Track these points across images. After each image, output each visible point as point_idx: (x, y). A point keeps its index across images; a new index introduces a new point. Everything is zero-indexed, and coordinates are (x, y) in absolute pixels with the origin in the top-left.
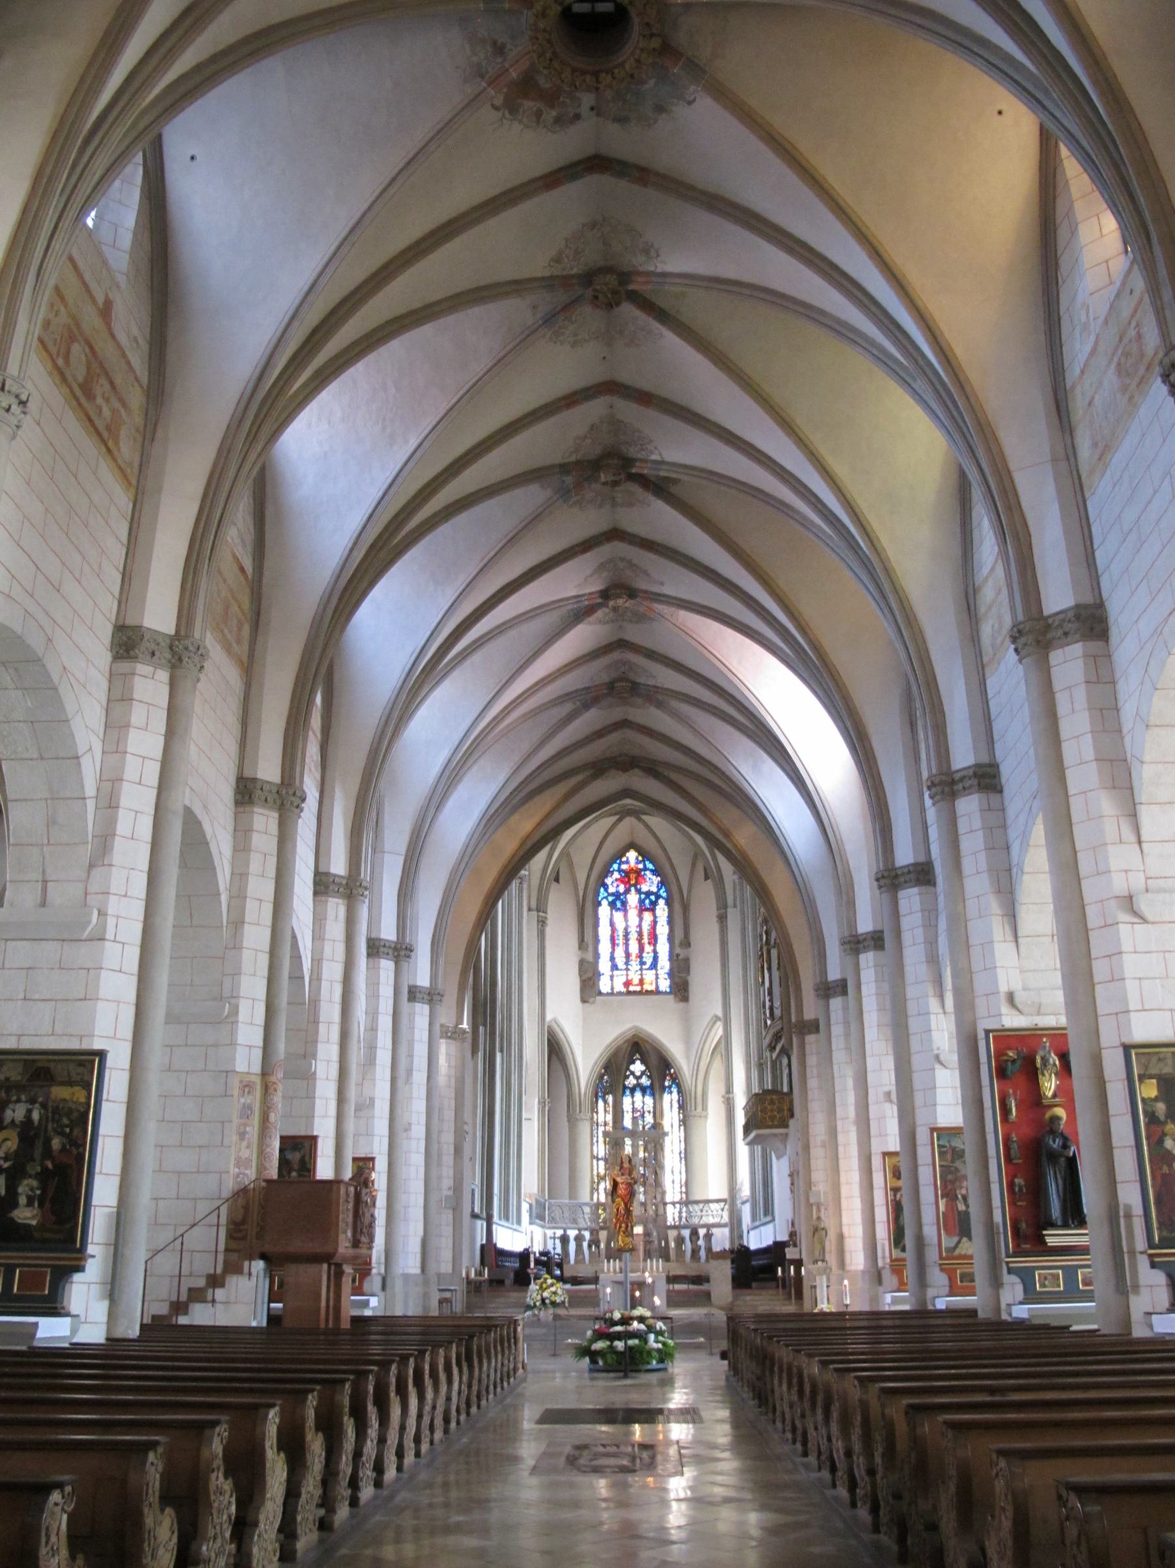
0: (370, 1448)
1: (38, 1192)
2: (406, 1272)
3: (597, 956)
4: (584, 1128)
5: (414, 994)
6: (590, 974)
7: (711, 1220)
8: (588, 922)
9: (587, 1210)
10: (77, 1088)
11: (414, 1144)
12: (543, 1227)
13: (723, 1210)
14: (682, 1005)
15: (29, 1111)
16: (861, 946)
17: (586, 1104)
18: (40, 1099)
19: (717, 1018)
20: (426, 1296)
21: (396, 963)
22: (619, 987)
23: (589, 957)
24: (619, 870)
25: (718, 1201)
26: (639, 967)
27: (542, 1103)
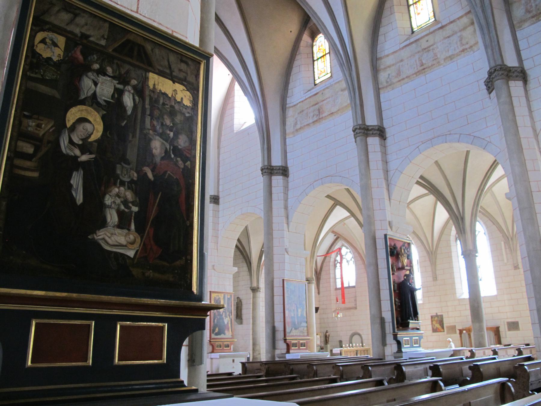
1: (135, 209)
15: (119, 93)
18: (134, 82)
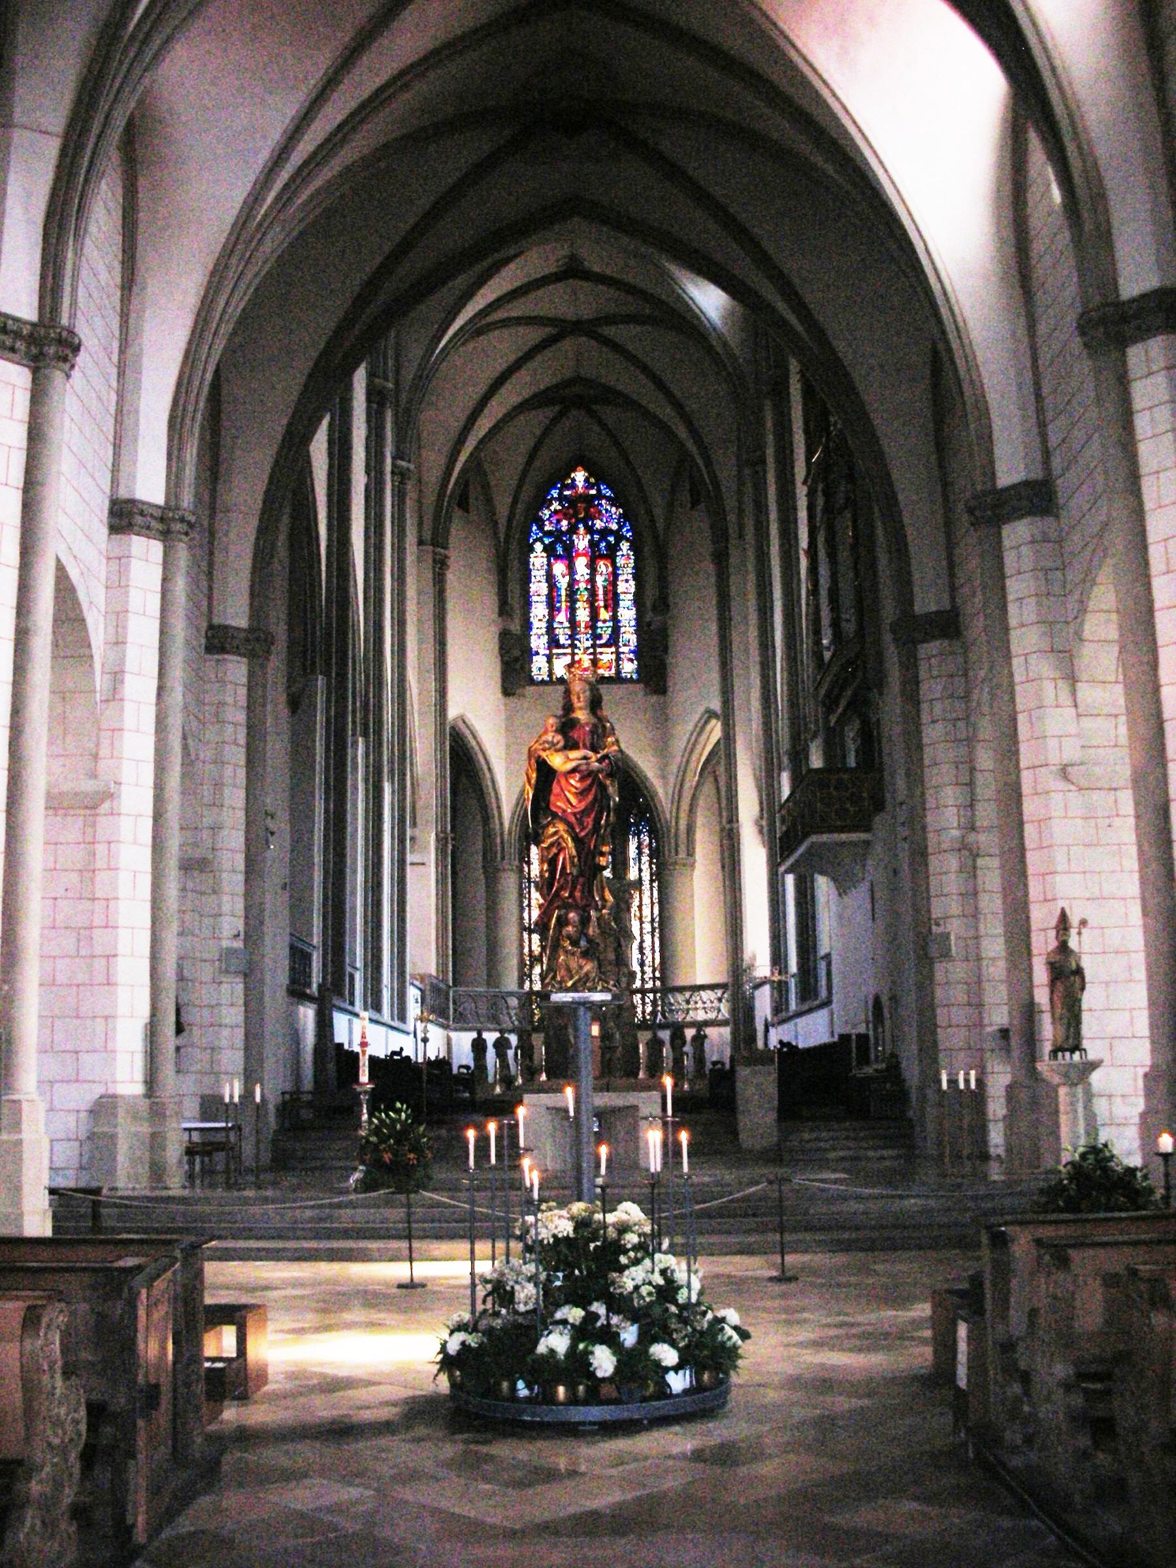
2: (110, 1092)
3: (527, 626)
4: (509, 882)
6: (516, 653)
7: (701, 1016)
8: (513, 575)
9: (514, 1002)
11: (126, 826)
12: (445, 1027)
13: (720, 1000)
14: (654, 699)
16: (1128, 330)
17: (512, 850)
19: (711, 714)
20: (156, 1142)
21: (35, 371)
22: (560, 670)
23: (515, 627)
24: (561, 499)
25: (712, 987)
26: (589, 643)
27: (441, 841)
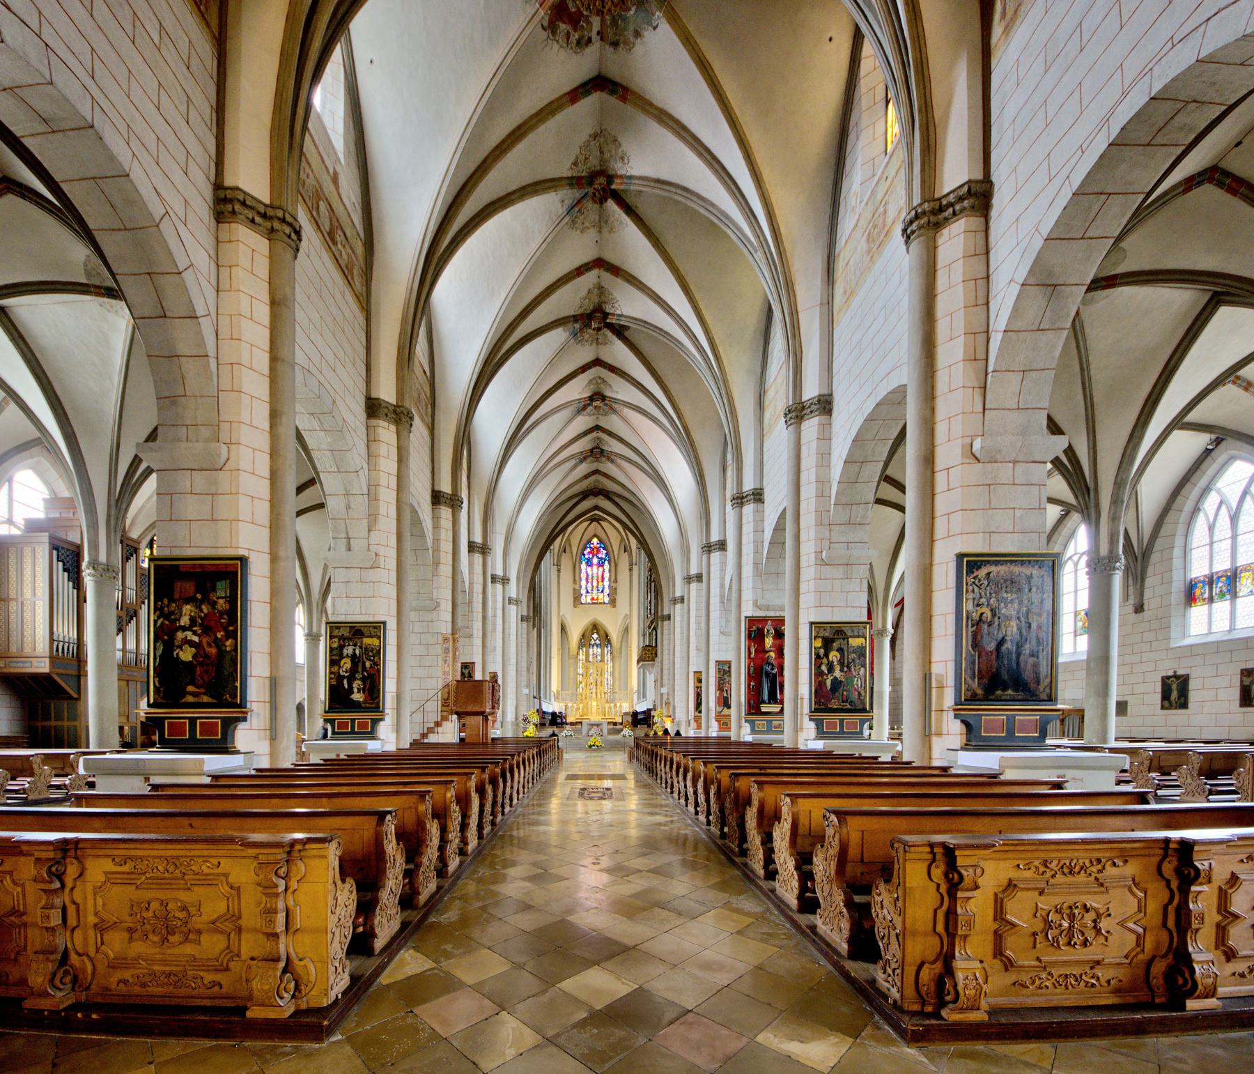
0: (508, 790)
5: (510, 600)
10: (374, 639)
22: (589, 600)
23: (577, 587)
